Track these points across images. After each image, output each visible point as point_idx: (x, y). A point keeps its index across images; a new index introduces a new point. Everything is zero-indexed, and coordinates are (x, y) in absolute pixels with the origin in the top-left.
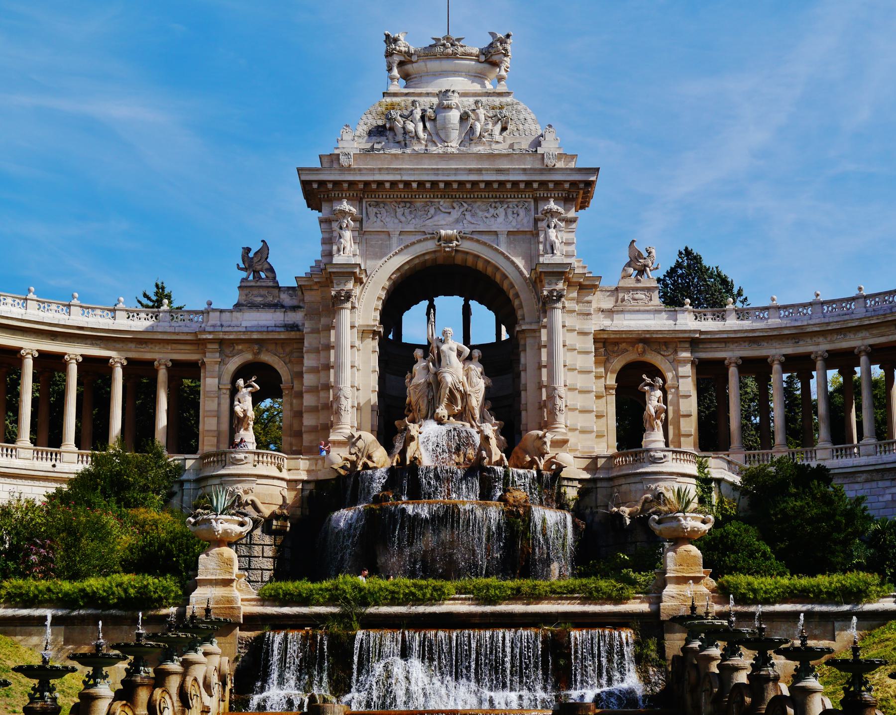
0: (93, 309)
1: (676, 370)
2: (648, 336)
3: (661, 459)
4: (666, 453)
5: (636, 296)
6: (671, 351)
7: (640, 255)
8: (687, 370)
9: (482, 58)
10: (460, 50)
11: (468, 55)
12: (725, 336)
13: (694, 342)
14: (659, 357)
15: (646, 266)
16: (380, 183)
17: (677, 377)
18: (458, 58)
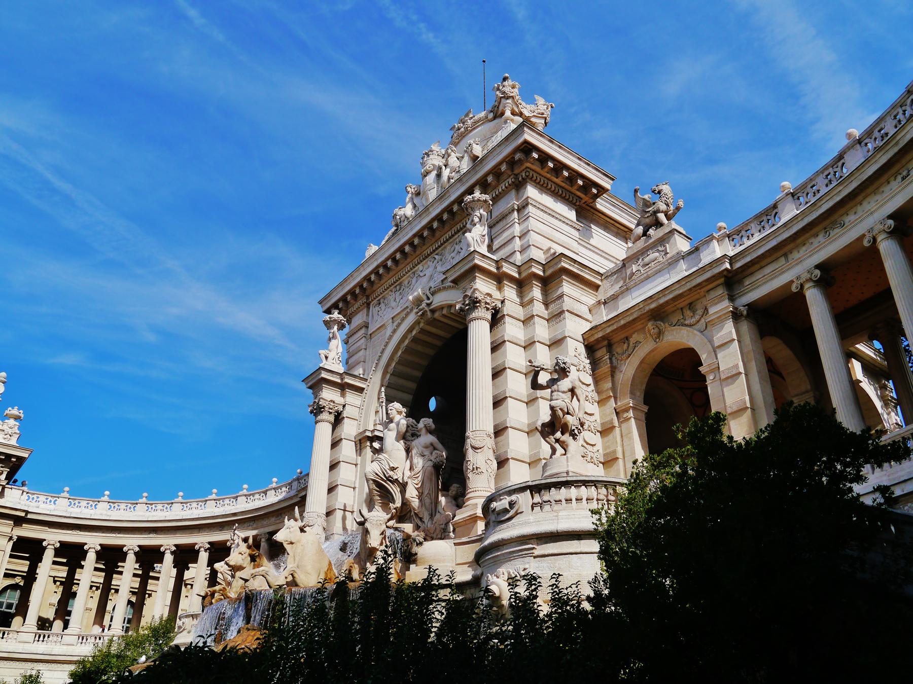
0: (253, 495)
1: (711, 342)
2: (653, 306)
3: (506, 511)
4: (514, 497)
5: (647, 260)
6: (700, 312)
7: (647, 204)
8: (729, 329)
9: (491, 116)
10: (470, 122)
11: (478, 122)
12: (774, 243)
13: (731, 279)
14: (684, 331)
15: (656, 212)
16: (367, 278)
17: (715, 350)
18: (471, 131)
